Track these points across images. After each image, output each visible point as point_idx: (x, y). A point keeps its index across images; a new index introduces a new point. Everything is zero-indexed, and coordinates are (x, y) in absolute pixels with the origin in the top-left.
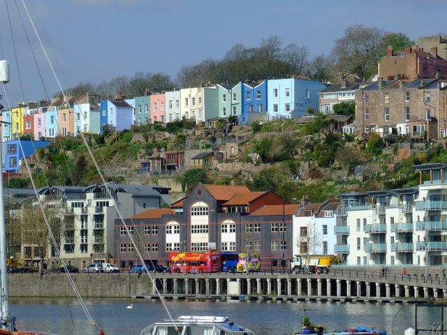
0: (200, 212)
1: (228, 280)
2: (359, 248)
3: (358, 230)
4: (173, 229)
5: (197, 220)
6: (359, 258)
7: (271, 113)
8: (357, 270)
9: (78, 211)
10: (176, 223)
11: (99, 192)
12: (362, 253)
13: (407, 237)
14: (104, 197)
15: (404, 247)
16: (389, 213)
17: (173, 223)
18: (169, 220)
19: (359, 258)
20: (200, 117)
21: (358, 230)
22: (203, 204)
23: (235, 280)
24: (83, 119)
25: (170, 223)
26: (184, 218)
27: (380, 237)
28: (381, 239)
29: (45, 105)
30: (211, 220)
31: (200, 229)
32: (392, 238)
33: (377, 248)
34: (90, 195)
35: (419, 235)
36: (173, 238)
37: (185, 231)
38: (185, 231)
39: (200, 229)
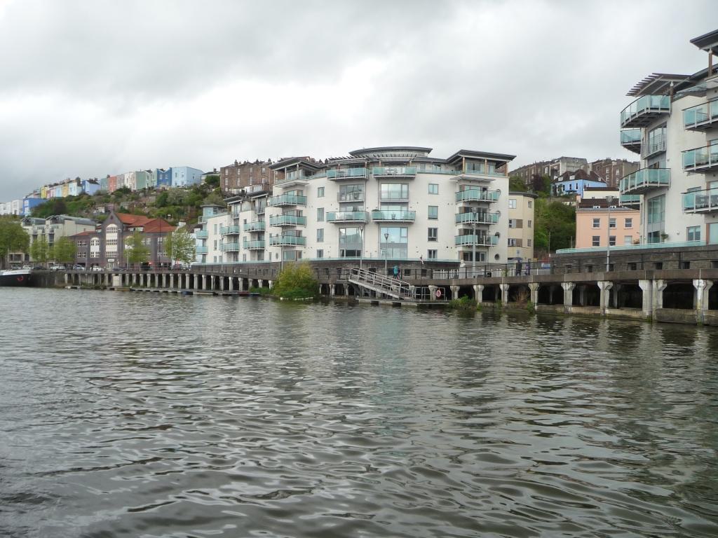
0: (112, 231)
1: (113, 275)
2: (216, 249)
3: (216, 234)
4: (95, 243)
5: (112, 236)
6: (215, 257)
7: (173, 185)
8: (212, 267)
9: (40, 232)
10: (97, 239)
11: (55, 221)
12: (218, 253)
13: (259, 234)
14: (57, 223)
15: (256, 244)
16: (242, 216)
17: (95, 239)
18: (94, 236)
19: (215, 257)
20: (134, 188)
21: (216, 234)
22: (114, 226)
23: (117, 275)
24: (74, 191)
25: (94, 239)
26: (102, 236)
27: (234, 236)
28: (234, 241)
29: (56, 185)
30: (119, 236)
31: (112, 242)
32: (245, 238)
33: (232, 247)
34: (48, 222)
35: (272, 232)
36: (95, 249)
37: (103, 244)
38: (103, 244)
39: (112, 242)
